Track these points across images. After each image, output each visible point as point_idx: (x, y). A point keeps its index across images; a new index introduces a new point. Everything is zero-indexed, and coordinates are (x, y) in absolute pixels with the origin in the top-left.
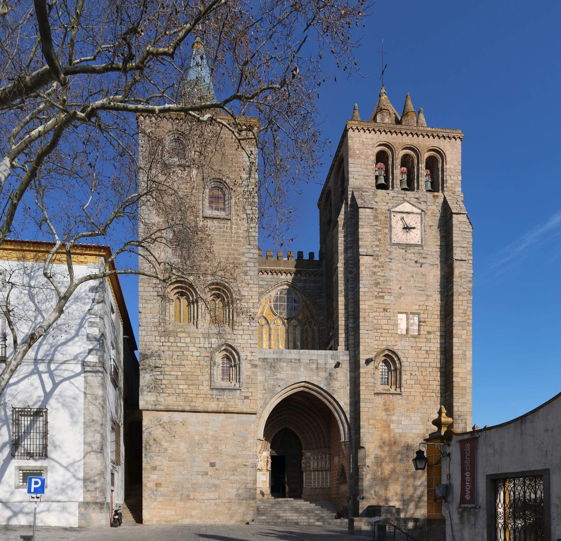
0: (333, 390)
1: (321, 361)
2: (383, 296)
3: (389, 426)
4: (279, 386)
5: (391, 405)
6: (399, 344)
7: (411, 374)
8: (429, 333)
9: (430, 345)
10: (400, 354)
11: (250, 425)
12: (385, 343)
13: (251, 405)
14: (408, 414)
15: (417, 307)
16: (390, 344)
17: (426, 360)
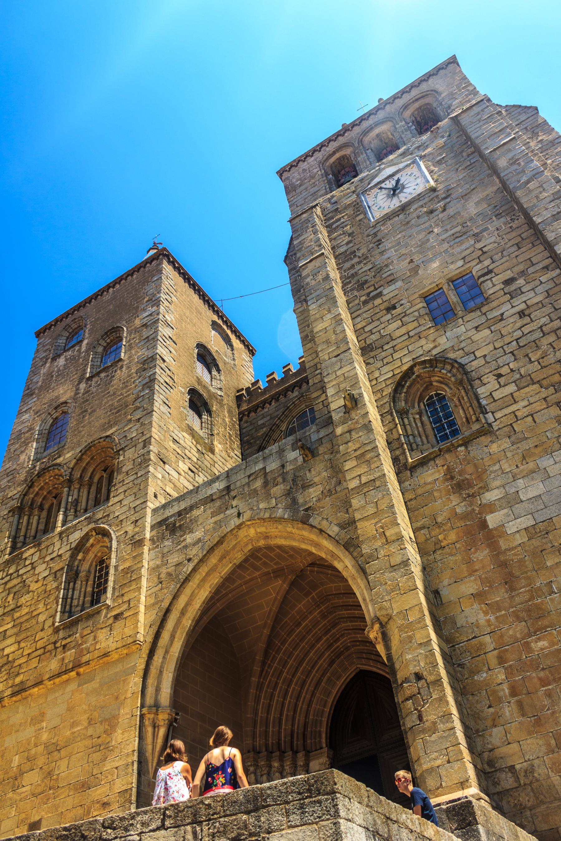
0: (306, 510)
1: (273, 465)
2: (381, 292)
3: (484, 524)
4: (189, 560)
5: (470, 469)
6: (442, 340)
7: (499, 376)
8: (508, 282)
9: (523, 298)
10: (452, 355)
11: (124, 681)
12: (405, 360)
13: (126, 630)
14: (531, 465)
15: (460, 263)
16: (421, 353)
17: (526, 330)
